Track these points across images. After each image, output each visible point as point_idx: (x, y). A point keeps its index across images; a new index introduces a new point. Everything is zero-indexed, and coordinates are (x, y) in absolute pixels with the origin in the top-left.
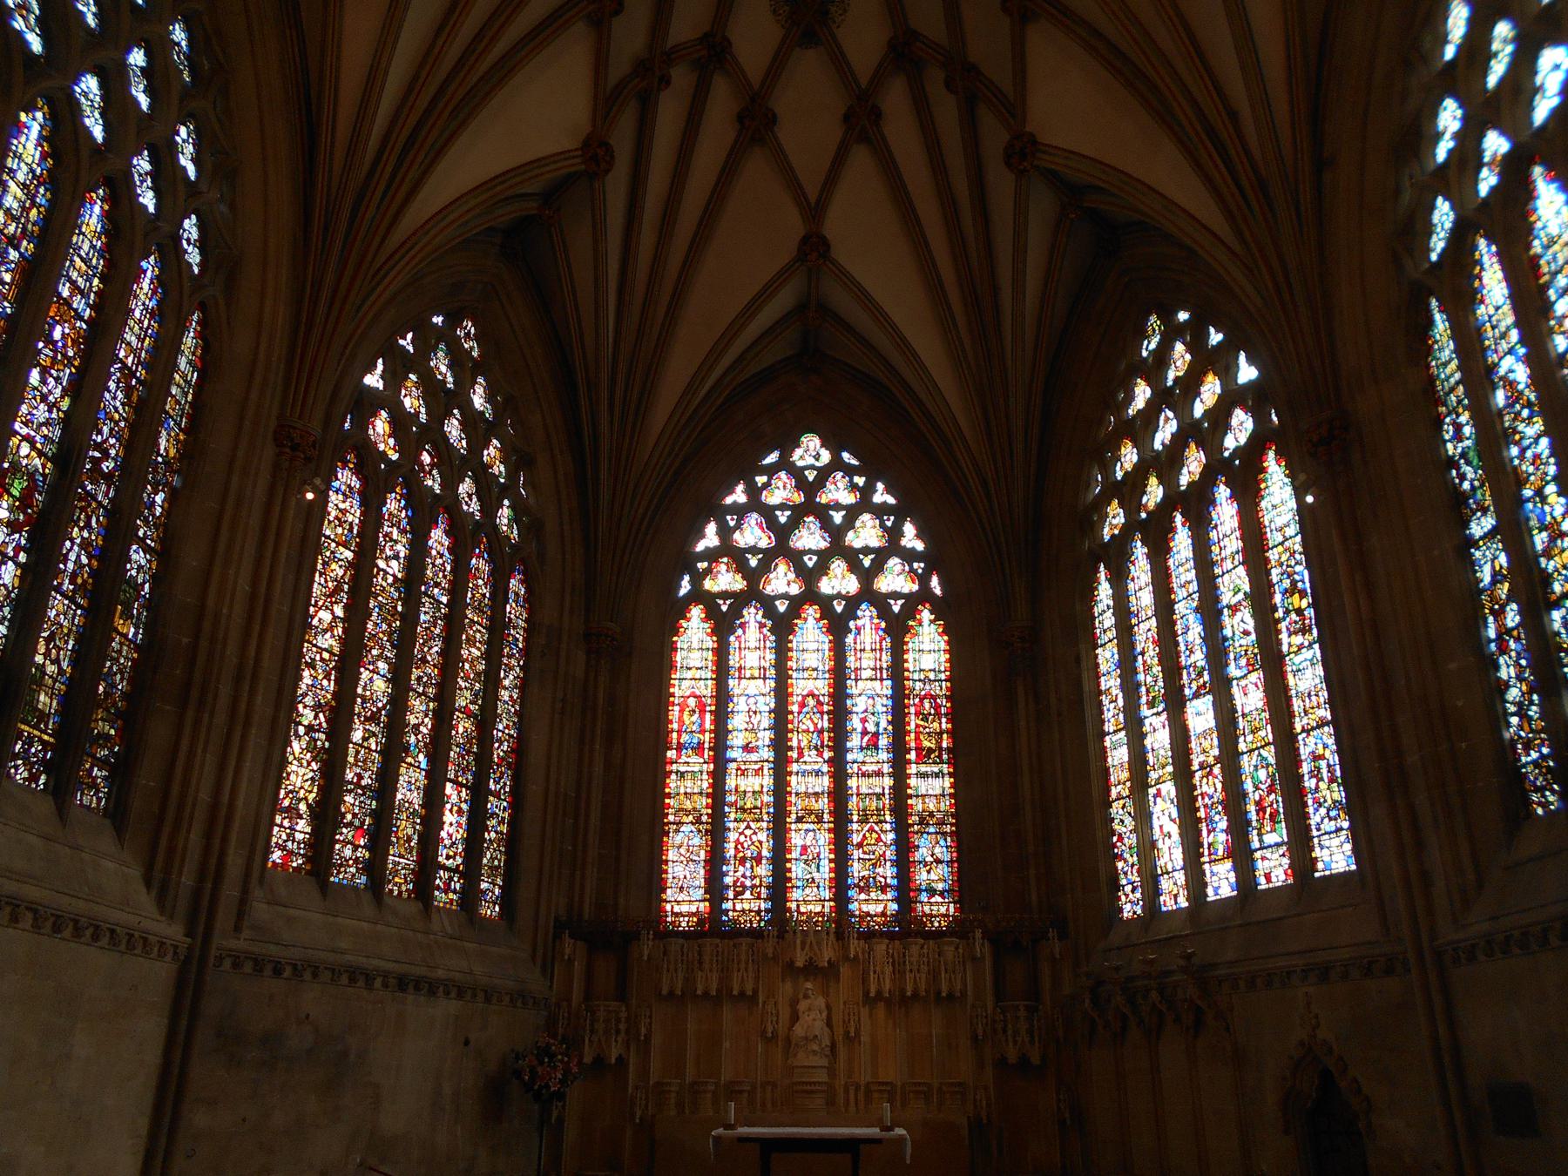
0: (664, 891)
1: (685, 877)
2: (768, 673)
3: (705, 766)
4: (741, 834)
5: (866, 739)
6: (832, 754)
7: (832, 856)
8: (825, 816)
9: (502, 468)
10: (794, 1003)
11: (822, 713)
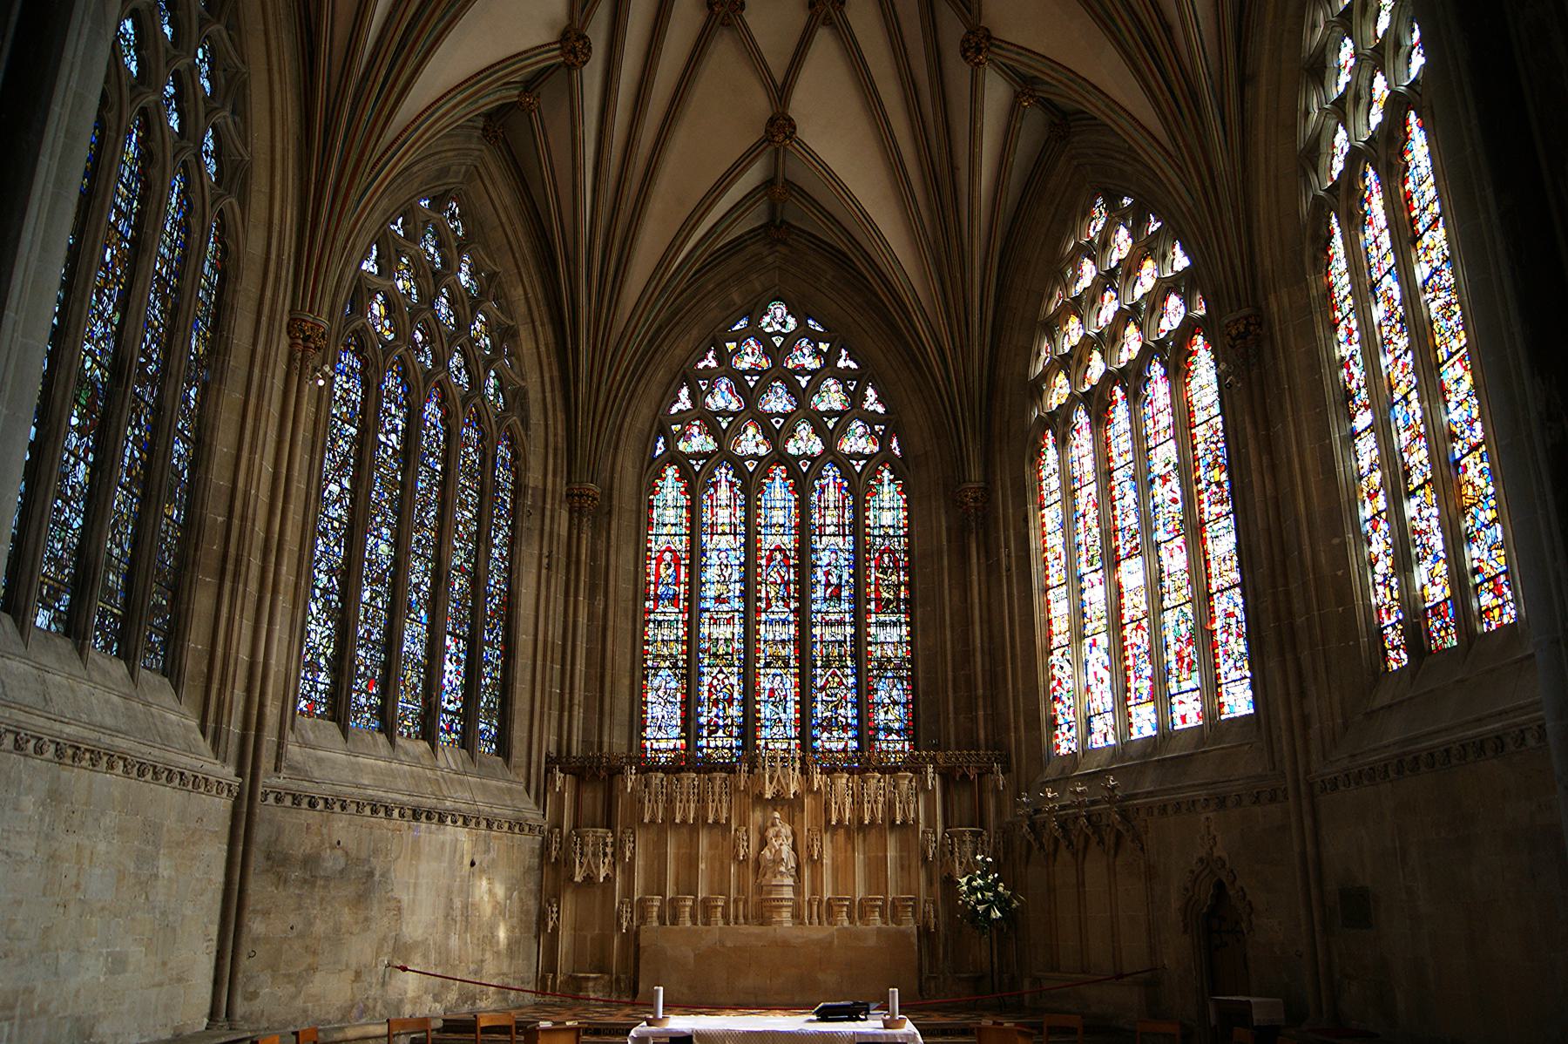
0: (644, 729)
3: (680, 616)
5: (829, 591)
6: (797, 604)
7: (798, 698)
9: (488, 342)
10: (762, 833)
11: (788, 566)
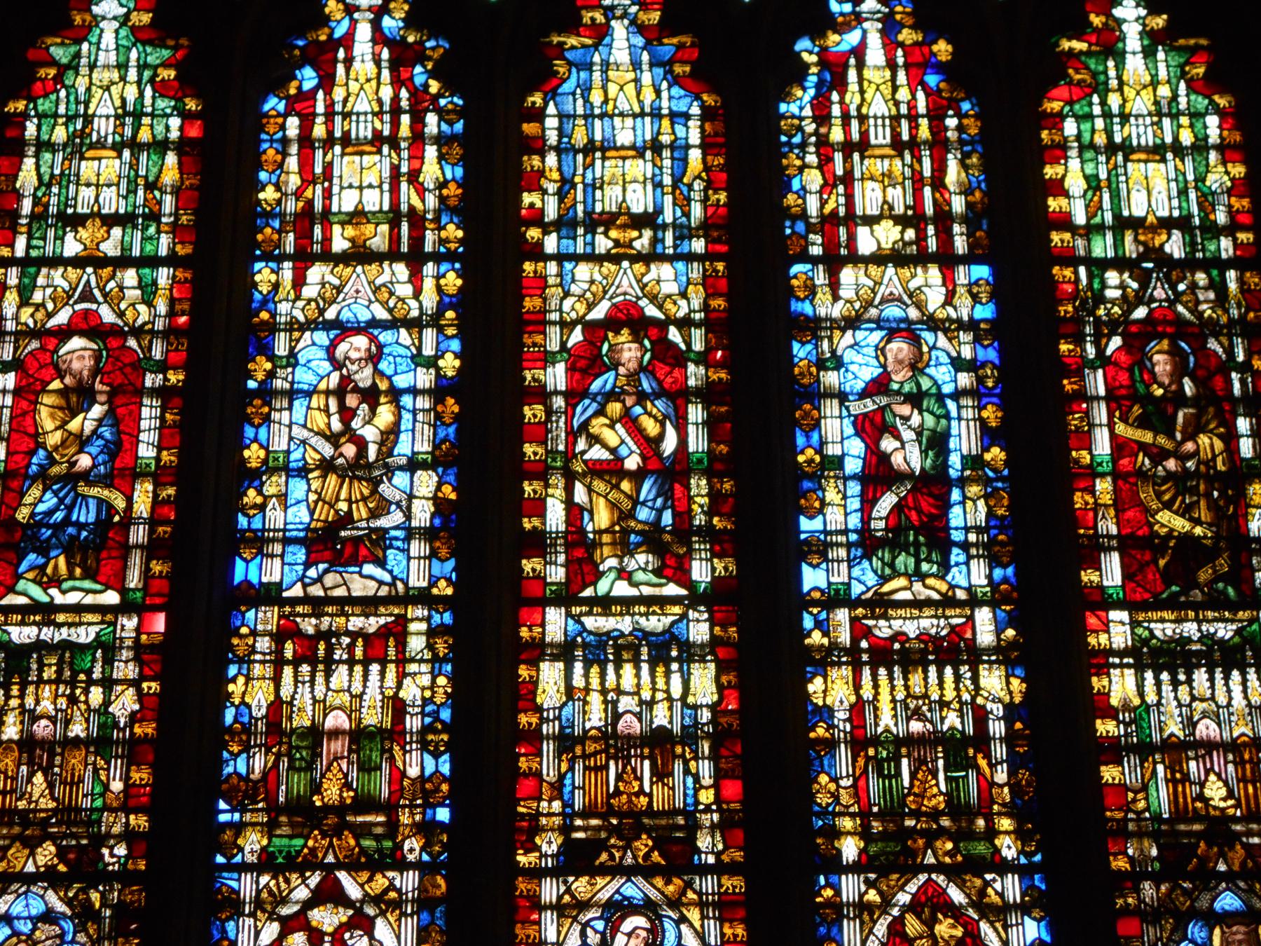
2: (430, 237)
3: (129, 624)
5: (887, 503)
8: (704, 842)
11: (679, 397)
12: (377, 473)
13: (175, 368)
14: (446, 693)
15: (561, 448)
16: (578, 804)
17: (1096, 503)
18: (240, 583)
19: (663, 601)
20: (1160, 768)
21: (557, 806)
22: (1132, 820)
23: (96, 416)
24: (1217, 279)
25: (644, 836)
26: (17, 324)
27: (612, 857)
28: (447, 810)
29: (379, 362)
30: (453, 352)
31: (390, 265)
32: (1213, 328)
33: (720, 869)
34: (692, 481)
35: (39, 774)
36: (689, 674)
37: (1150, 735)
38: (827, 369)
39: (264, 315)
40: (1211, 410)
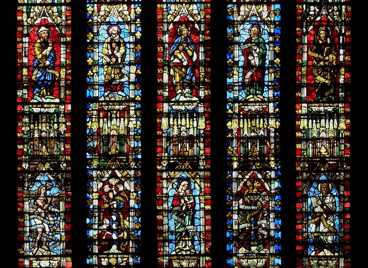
0: (21, 243)
1: (44, 230)
3: (62, 107)
4: (105, 183)
5: (249, 74)
7: (208, 207)
8: (201, 163)
11: (197, 45)
12: (121, 66)
13: (68, 36)
14: (139, 126)
15: (167, 59)
16: (171, 154)
17: (302, 74)
18: (88, 97)
19: (193, 102)
20: (311, 145)
21: (166, 154)
22: (302, 158)
23: (50, 50)
24: (340, 8)
25: (187, 162)
26: (27, 23)
27: (179, 167)
28: (140, 156)
29: (120, 34)
30: (139, 31)
31: (122, 5)
32: (336, 23)
33: (204, 170)
34: (200, 69)
35: (44, 146)
36: (198, 121)
37: (309, 136)
38: (236, 36)
39: (90, 20)
40: (334, 47)
